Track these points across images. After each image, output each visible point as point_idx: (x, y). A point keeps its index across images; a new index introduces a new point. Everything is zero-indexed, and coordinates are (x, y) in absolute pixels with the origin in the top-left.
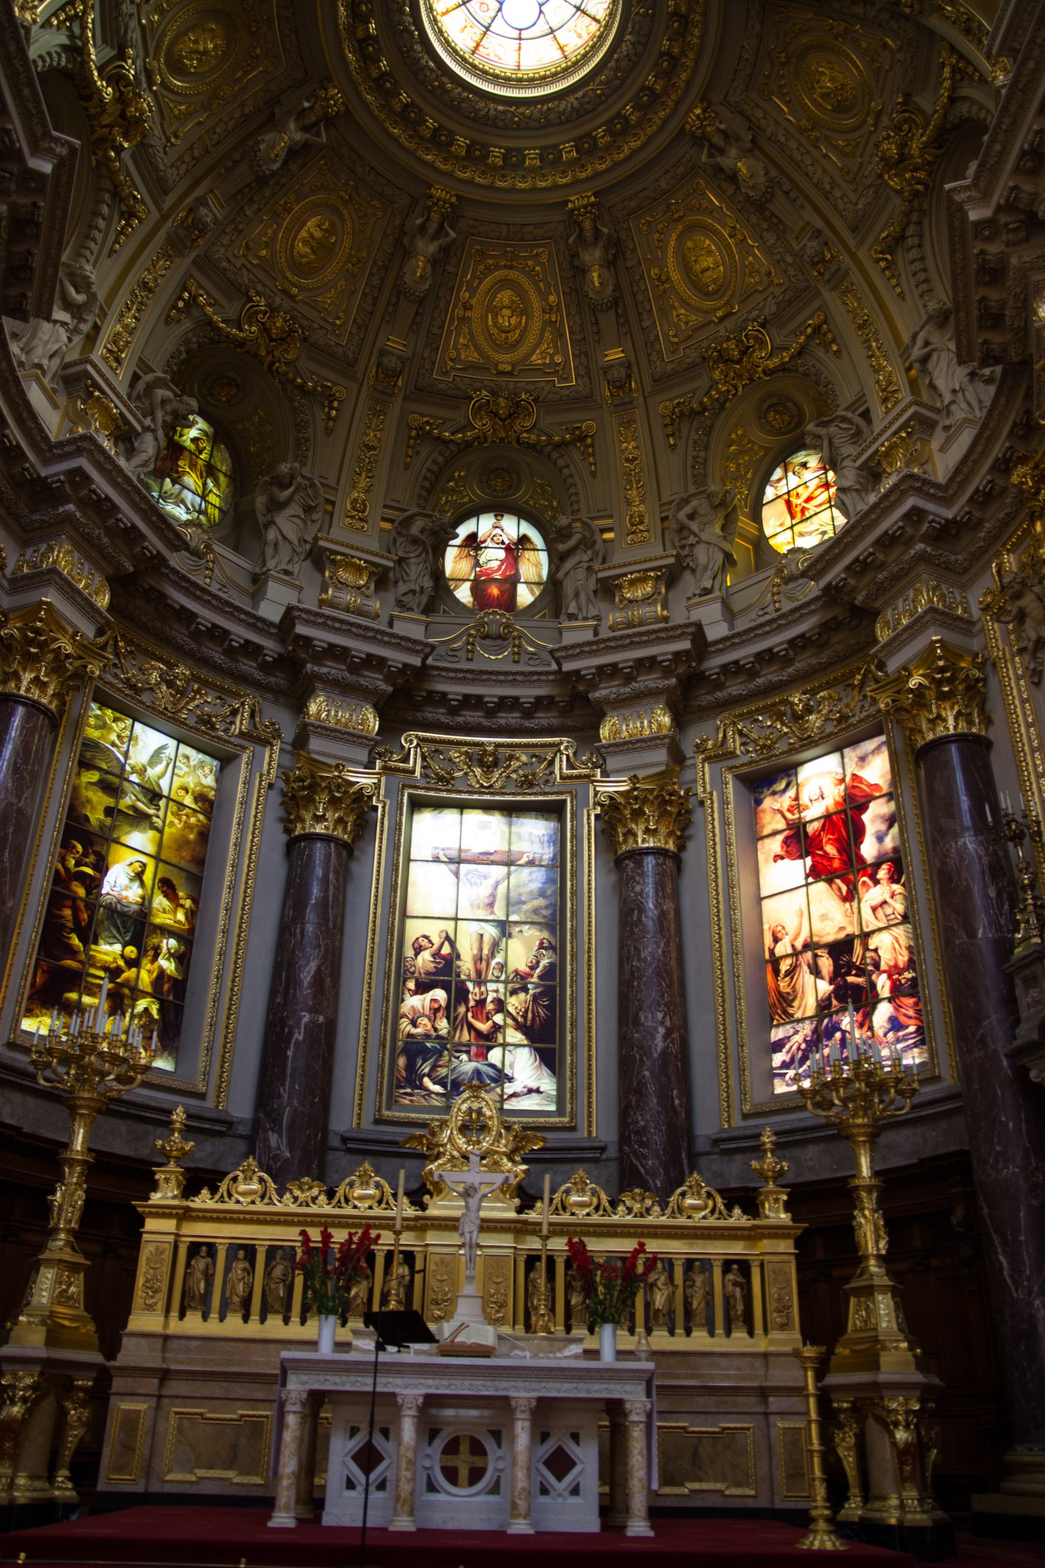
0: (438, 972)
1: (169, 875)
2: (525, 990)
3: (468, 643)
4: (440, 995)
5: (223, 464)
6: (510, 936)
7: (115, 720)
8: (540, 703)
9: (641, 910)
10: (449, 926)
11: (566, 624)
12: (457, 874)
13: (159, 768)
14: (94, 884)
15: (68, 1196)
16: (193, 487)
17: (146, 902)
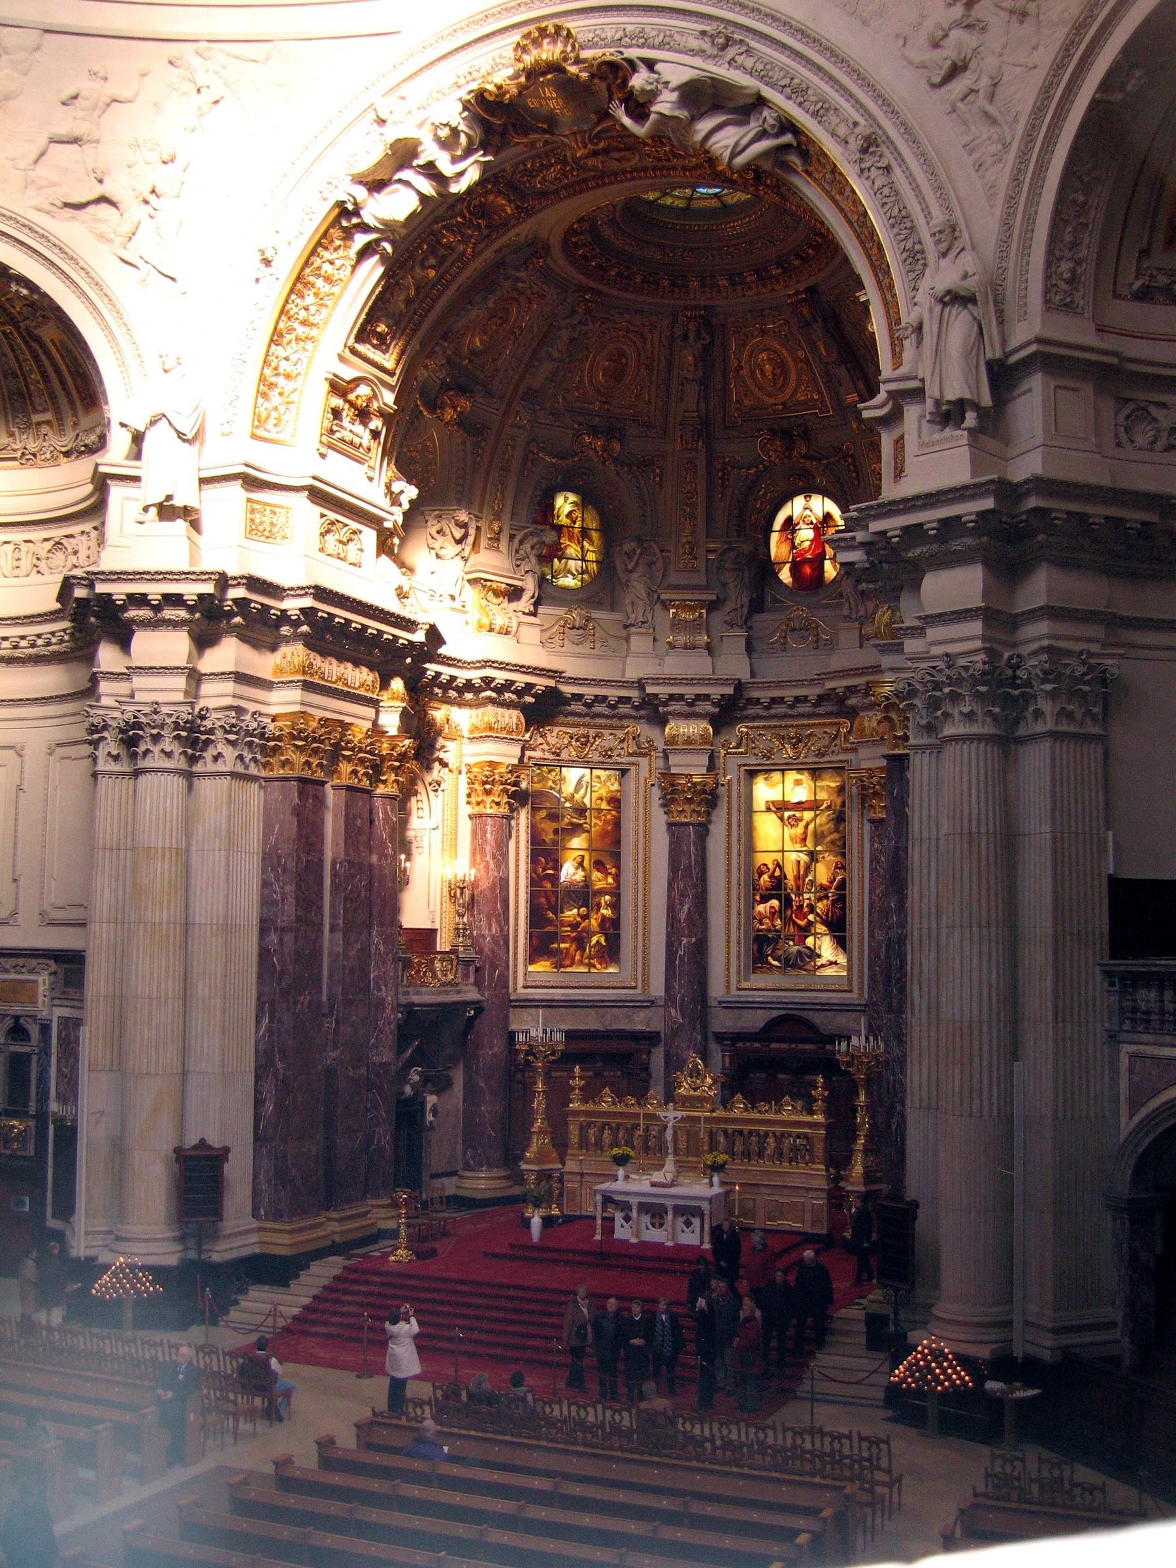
0: (773, 888)
1: (598, 857)
2: (827, 897)
3: (780, 636)
4: (775, 903)
5: (592, 523)
6: (817, 861)
7: (549, 772)
8: (821, 698)
9: (878, 861)
10: (778, 856)
11: (842, 625)
12: (781, 818)
13: (582, 792)
14: (555, 879)
15: (539, 1104)
16: (574, 555)
17: (587, 878)
